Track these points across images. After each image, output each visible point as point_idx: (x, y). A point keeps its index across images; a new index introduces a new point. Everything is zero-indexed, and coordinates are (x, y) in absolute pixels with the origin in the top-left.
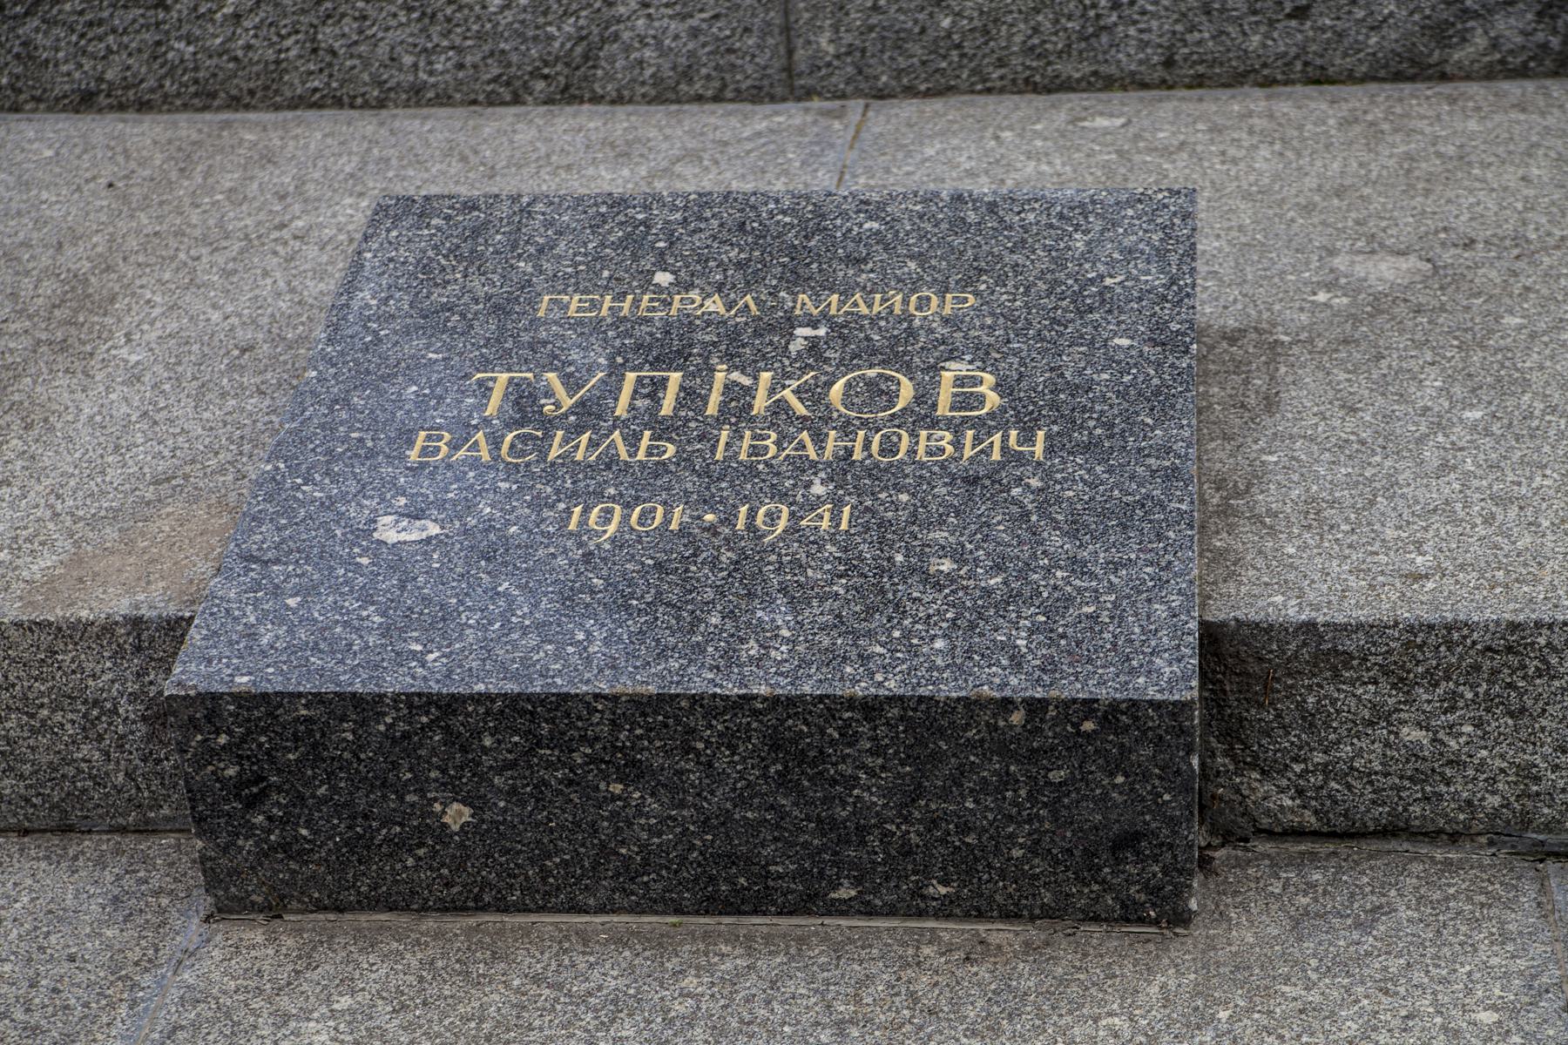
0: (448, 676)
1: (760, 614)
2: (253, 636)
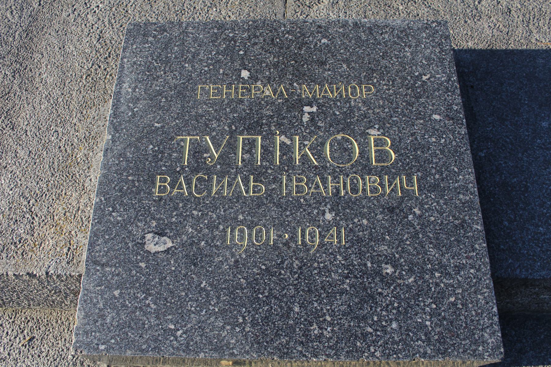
0: (187, 347)
1: (316, 305)
2: (103, 317)
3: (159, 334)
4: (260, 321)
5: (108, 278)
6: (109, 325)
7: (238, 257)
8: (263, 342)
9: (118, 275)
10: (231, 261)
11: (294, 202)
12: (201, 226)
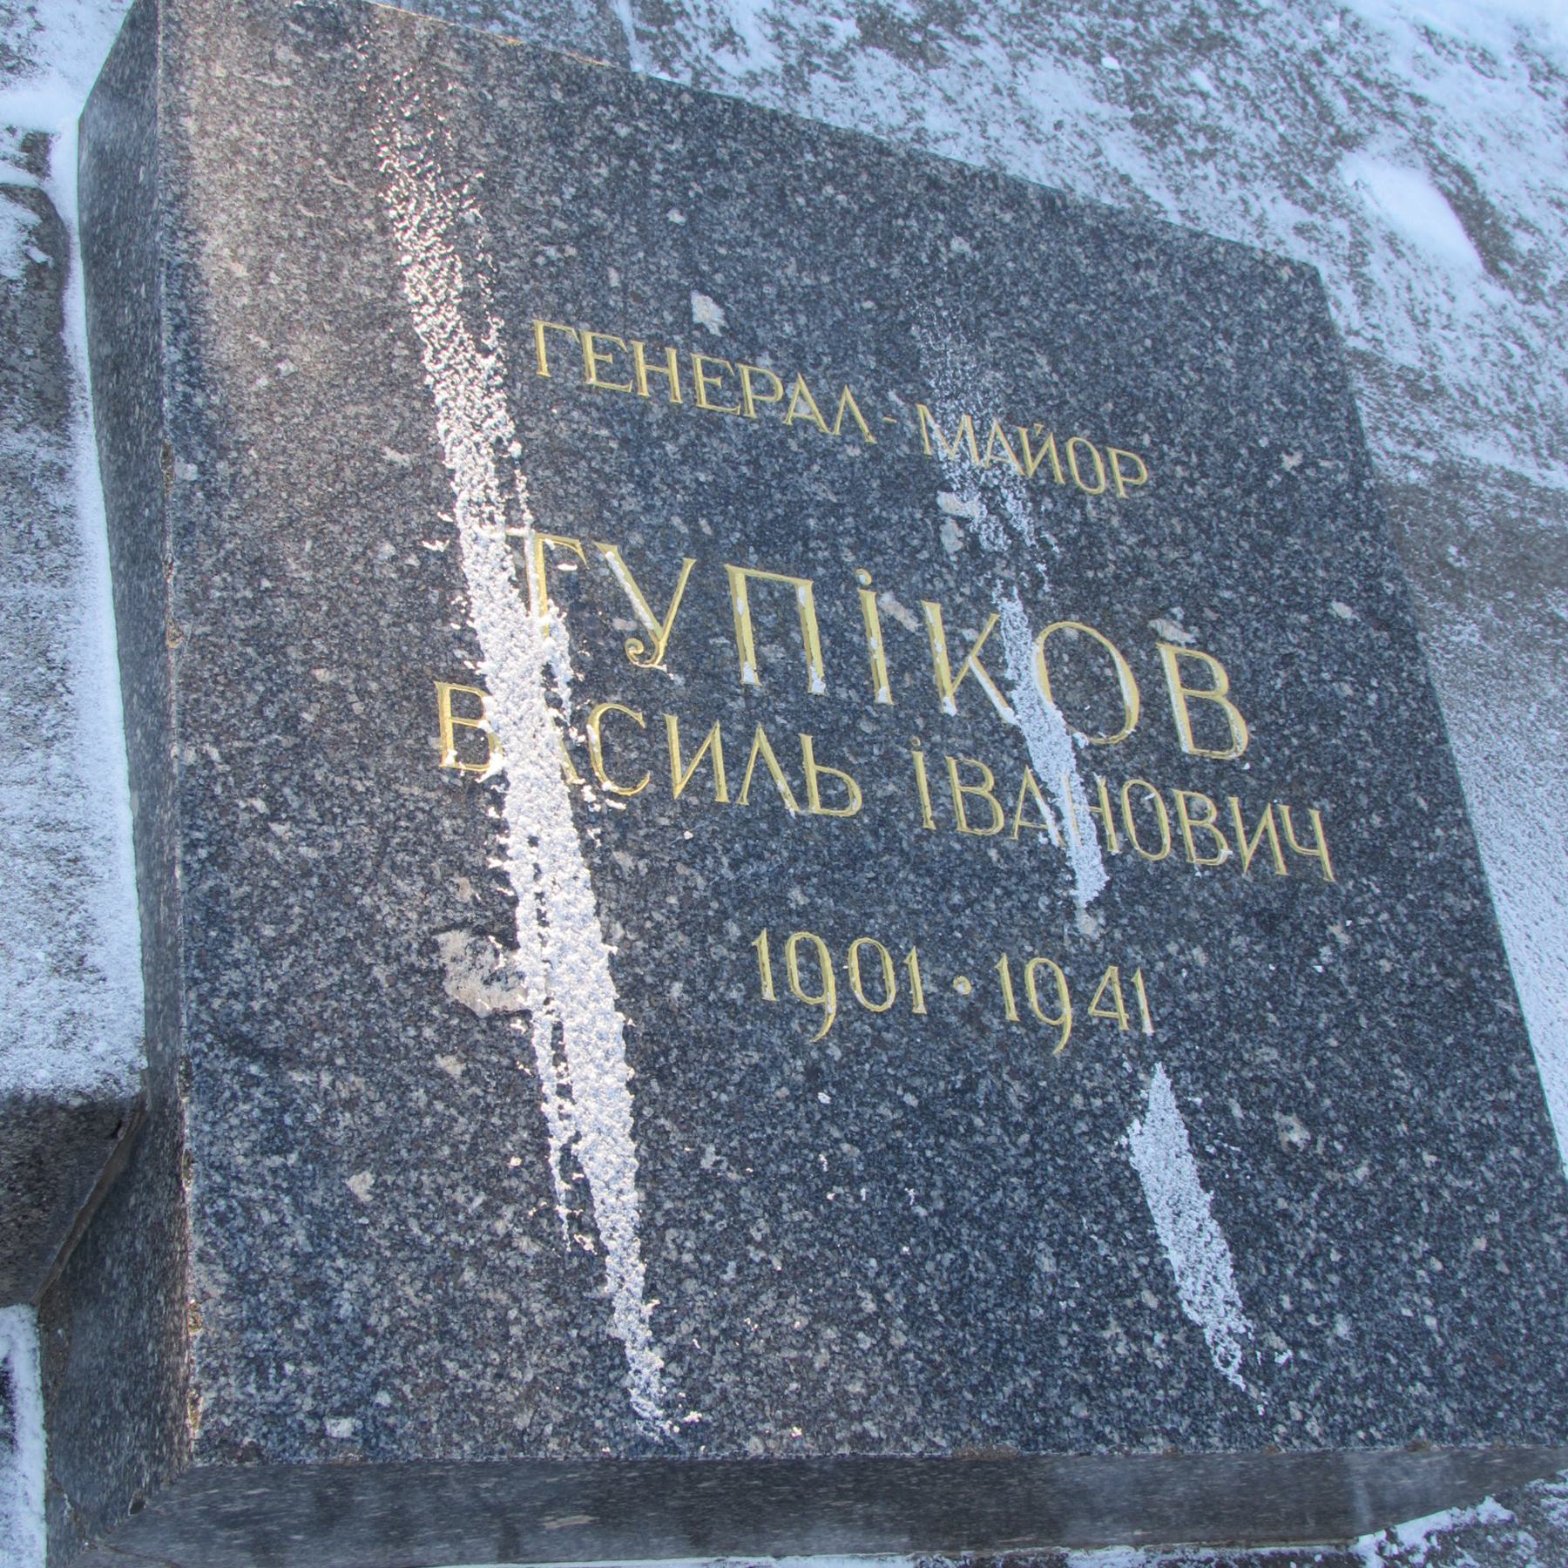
3: (572, 1365)
4: (936, 1308)
5: (310, 1118)
6: (356, 1331)
7: (815, 1054)
8: (959, 1389)
9: (350, 1104)
10: (794, 1070)
11: (968, 856)
12: (657, 916)
